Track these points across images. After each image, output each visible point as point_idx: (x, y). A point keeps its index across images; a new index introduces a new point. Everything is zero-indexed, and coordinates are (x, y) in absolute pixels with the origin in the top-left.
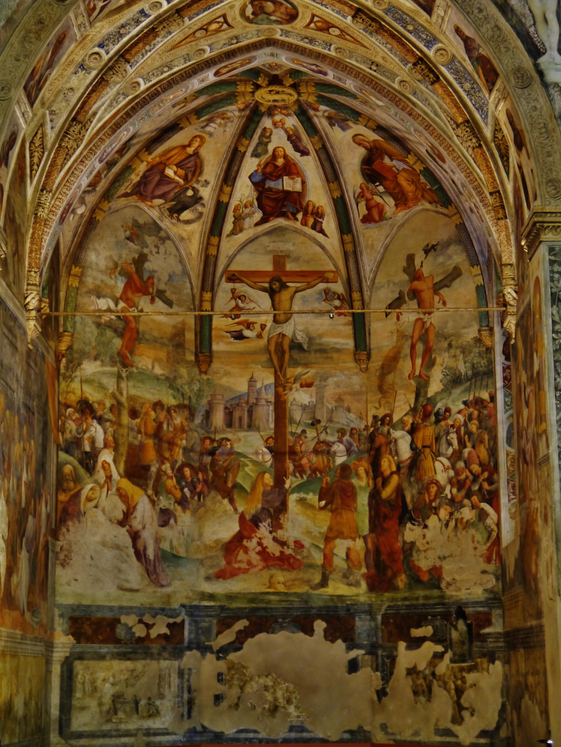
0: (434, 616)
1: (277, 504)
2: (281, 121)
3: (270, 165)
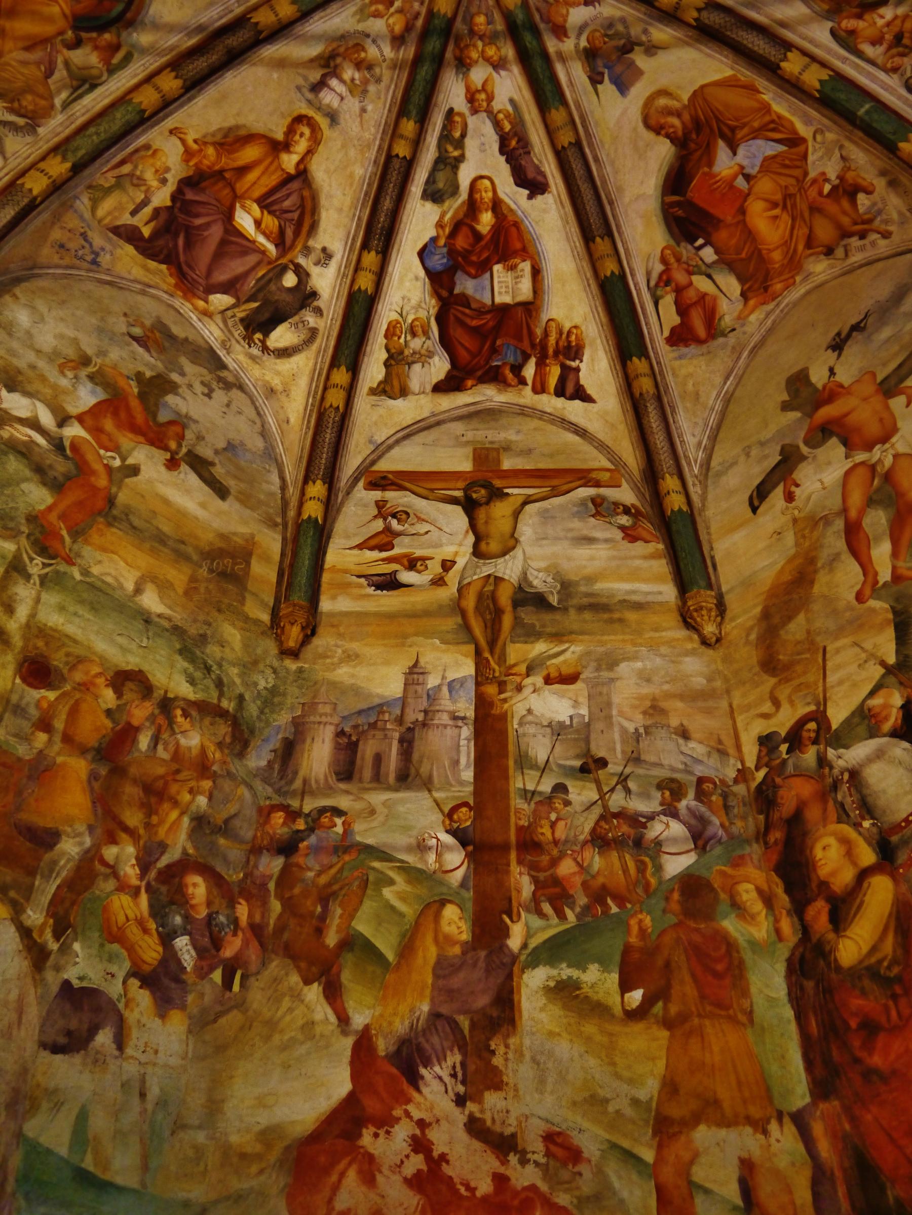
1: (482, 1001)
2: (484, 89)
3: (465, 230)
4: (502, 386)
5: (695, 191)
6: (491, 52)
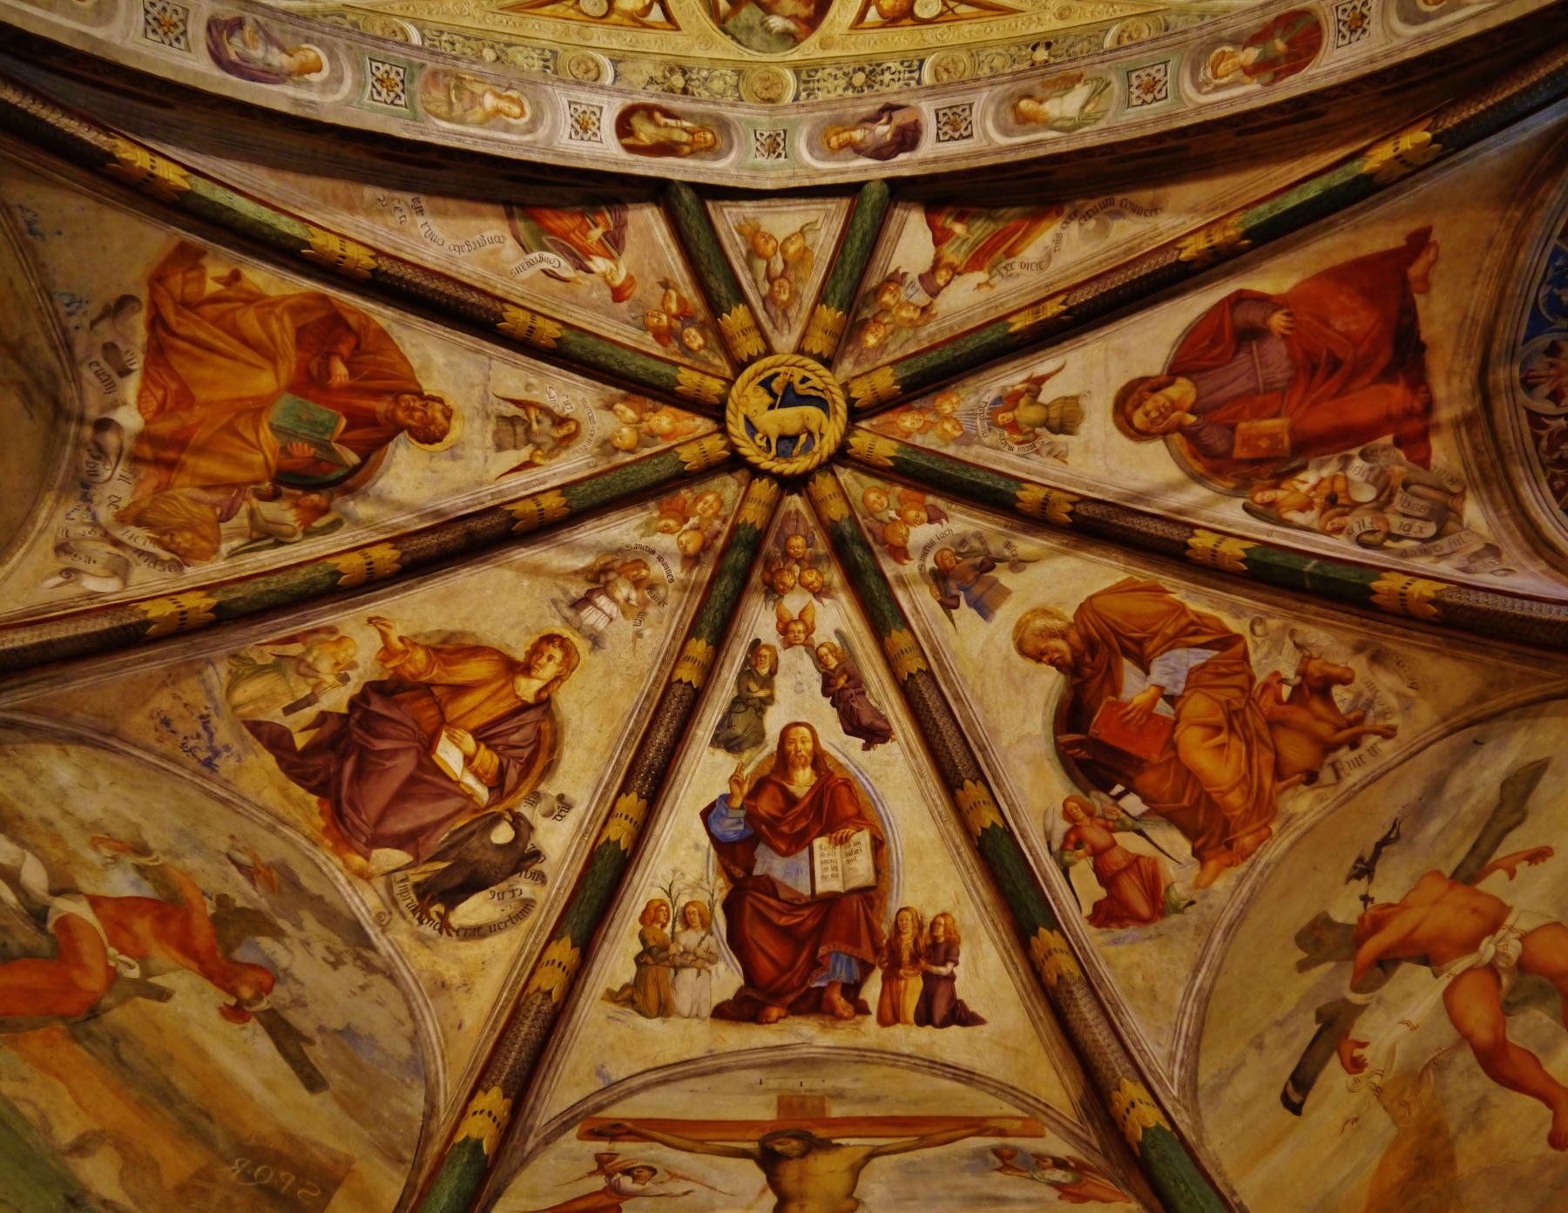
2: (801, 618)
3: (771, 790)
4: (827, 1021)
5: (1099, 726)
6: (811, 577)
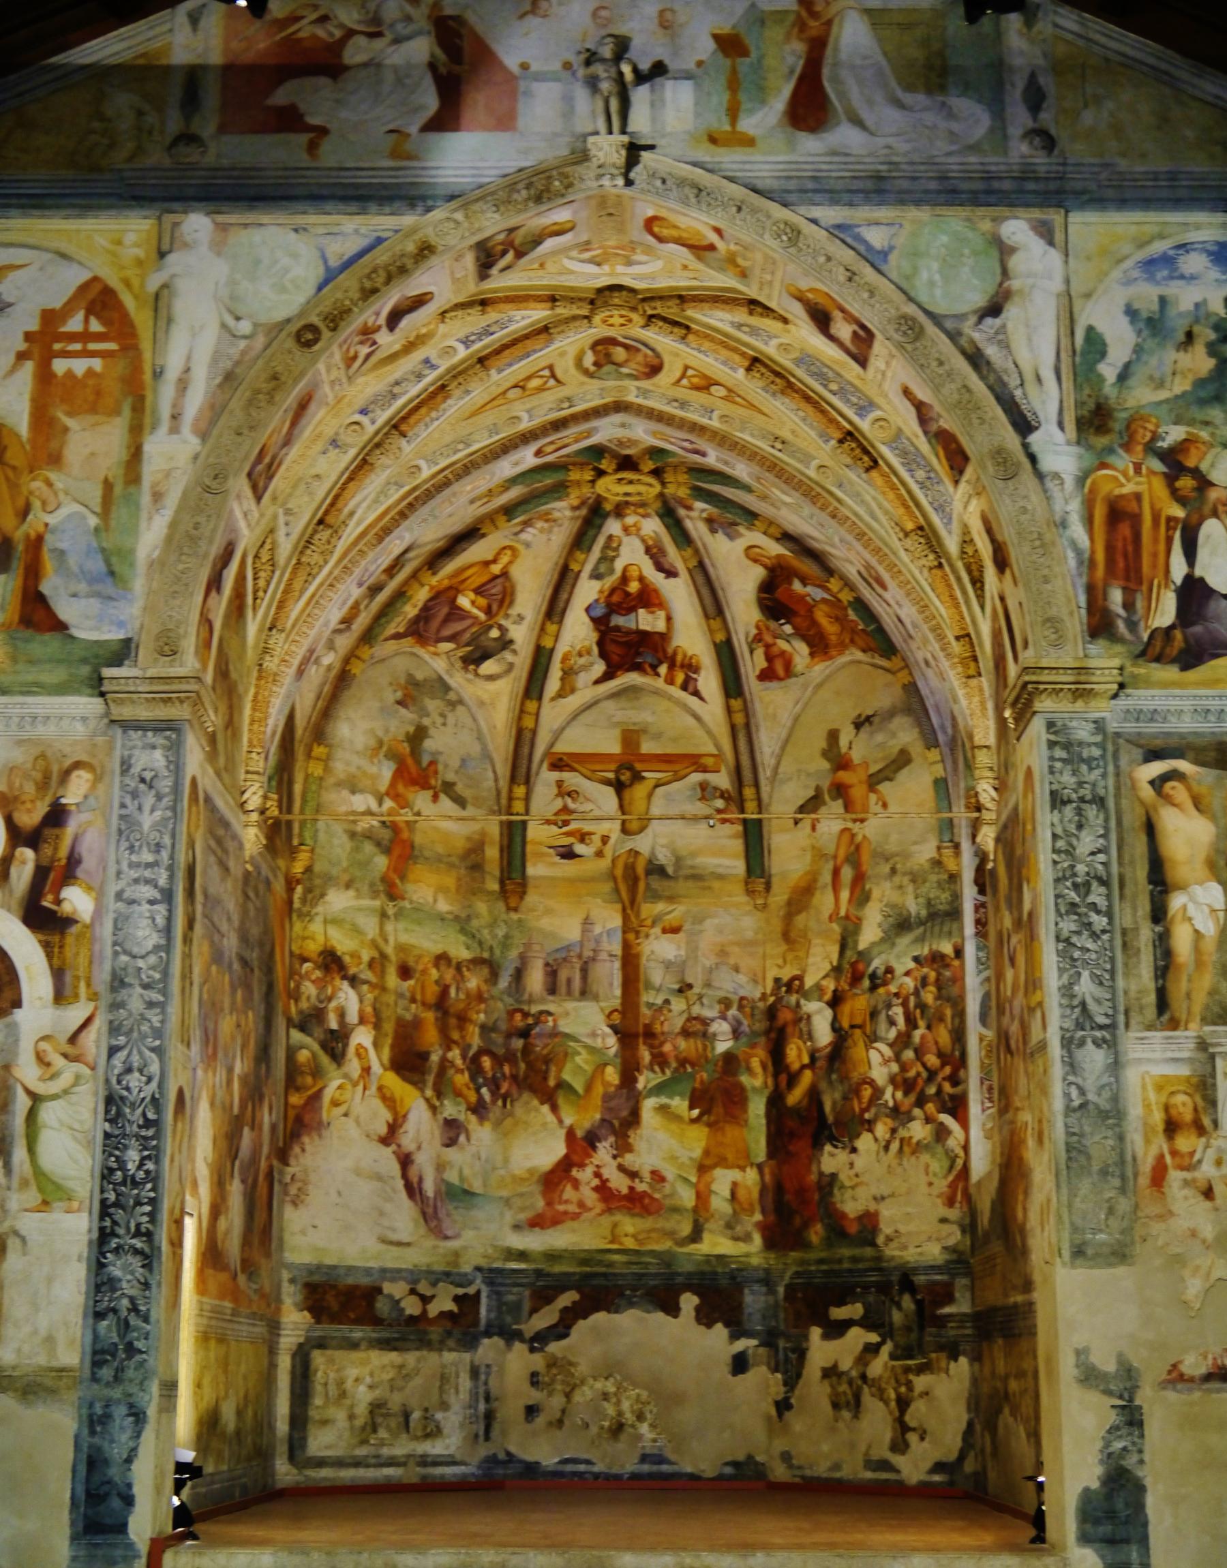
0: (866, 1287)
1: (625, 1113)
5: (780, 593)
